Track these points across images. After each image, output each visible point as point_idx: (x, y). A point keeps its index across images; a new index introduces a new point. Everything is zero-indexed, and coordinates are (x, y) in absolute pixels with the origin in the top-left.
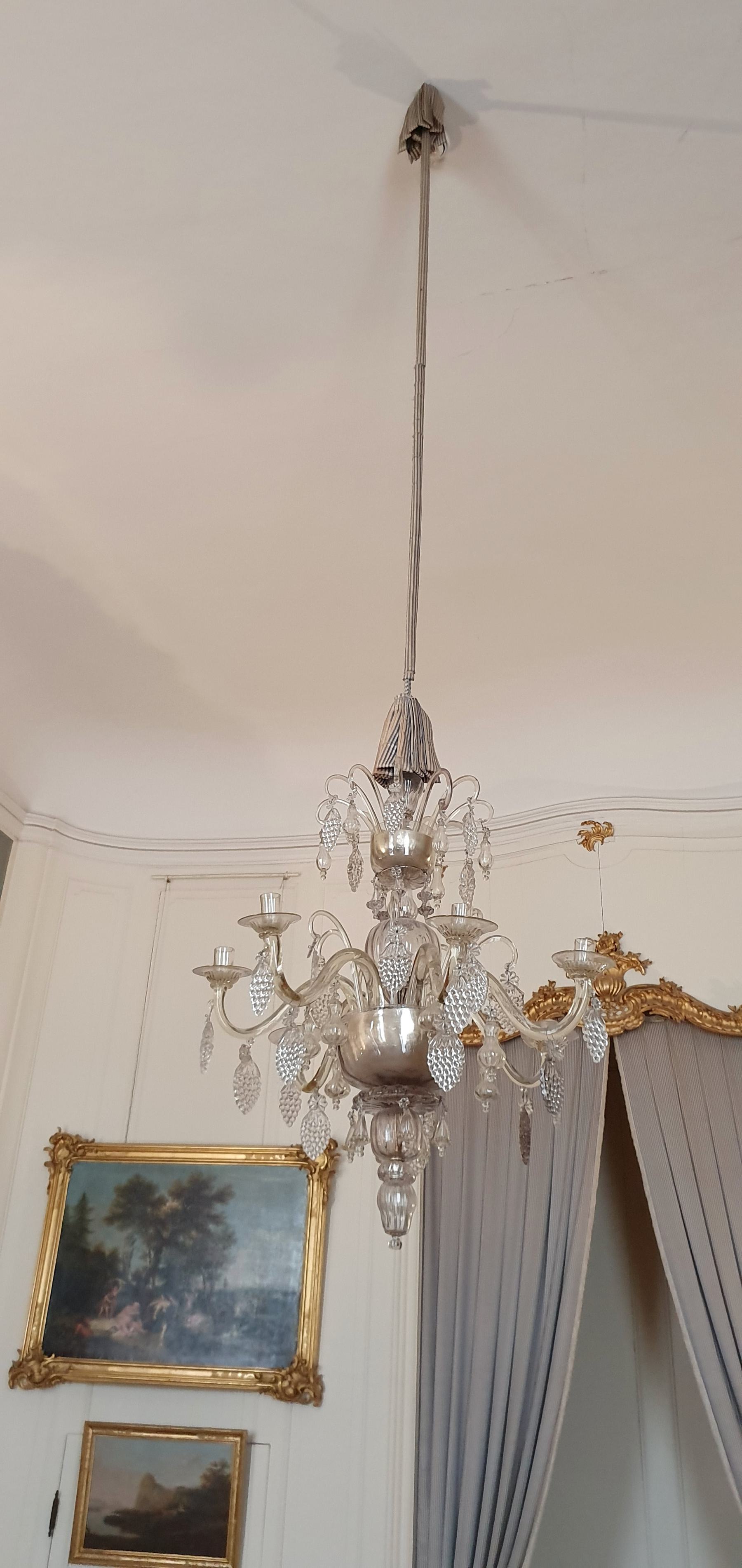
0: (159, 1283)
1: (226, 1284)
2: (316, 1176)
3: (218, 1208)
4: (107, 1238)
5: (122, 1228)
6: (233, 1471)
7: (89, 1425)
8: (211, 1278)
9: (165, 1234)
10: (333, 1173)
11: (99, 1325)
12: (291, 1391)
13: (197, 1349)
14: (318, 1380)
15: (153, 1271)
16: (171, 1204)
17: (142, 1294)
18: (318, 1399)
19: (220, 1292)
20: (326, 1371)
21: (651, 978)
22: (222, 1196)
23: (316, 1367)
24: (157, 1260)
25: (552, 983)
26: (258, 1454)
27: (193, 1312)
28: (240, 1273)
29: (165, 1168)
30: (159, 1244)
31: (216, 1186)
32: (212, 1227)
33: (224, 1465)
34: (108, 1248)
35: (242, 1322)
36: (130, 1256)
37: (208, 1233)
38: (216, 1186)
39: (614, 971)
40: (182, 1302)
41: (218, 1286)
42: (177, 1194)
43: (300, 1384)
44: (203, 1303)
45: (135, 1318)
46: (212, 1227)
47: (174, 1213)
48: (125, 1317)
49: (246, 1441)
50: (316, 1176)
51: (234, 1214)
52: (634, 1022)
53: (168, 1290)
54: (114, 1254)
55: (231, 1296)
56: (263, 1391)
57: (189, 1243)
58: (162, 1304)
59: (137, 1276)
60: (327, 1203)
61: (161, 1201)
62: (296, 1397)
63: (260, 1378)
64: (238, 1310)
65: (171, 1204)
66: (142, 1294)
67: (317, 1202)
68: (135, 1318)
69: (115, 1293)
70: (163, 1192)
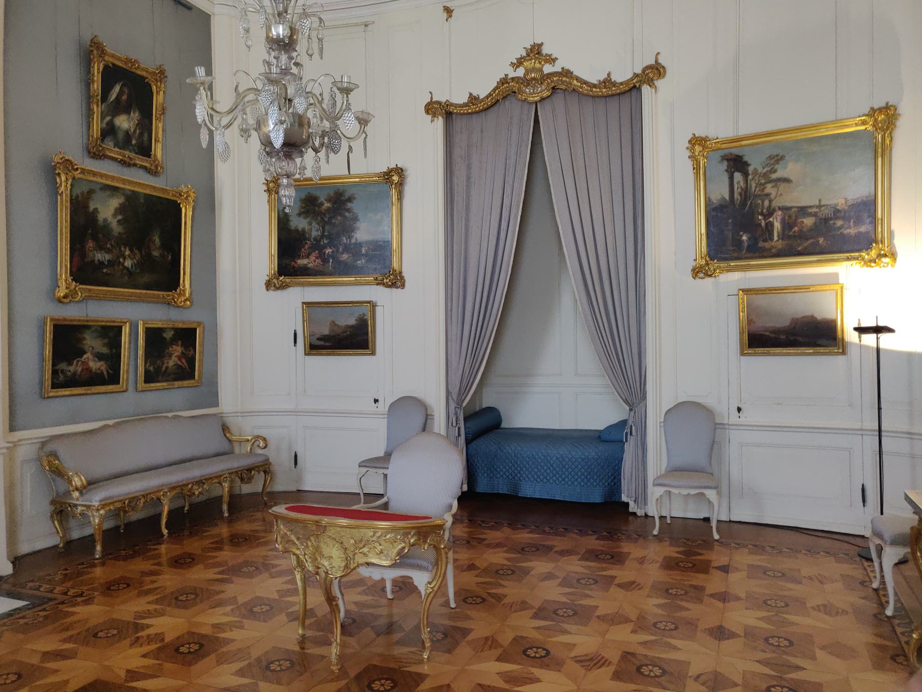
3: (349, 205)
4: (299, 223)
6: (368, 317)
7: (303, 303)
8: (350, 237)
9: (326, 219)
11: (302, 262)
13: (345, 269)
14: (402, 278)
15: (323, 236)
16: (327, 205)
17: (317, 246)
19: (356, 244)
21: (557, 68)
22: (350, 200)
23: (401, 273)
25: (506, 75)
26: (379, 310)
27: (342, 253)
28: (363, 233)
30: (323, 224)
31: (347, 195)
32: (347, 214)
33: (364, 315)
35: (366, 255)
38: (347, 195)
39: (537, 65)
41: (353, 241)
42: (329, 200)
43: (395, 280)
44: (347, 249)
46: (347, 214)
47: (328, 209)
48: (312, 258)
49: (373, 305)
51: (355, 206)
52: (546, 94)
53: (330, 245)
54: (303, 230)
55: (359, 245)
56: (378, 284)
58: (328, 251)
59: (315, 239)
60: (400, 198)
61: (322, 204)
62: (393, 285)
63: (376, 279)
64: (363, 251)
65: (327, 205)
66: (317, 246)
67: (395, 198)
68: (317, 258)
69: (306, 247)
70: (322, 199)
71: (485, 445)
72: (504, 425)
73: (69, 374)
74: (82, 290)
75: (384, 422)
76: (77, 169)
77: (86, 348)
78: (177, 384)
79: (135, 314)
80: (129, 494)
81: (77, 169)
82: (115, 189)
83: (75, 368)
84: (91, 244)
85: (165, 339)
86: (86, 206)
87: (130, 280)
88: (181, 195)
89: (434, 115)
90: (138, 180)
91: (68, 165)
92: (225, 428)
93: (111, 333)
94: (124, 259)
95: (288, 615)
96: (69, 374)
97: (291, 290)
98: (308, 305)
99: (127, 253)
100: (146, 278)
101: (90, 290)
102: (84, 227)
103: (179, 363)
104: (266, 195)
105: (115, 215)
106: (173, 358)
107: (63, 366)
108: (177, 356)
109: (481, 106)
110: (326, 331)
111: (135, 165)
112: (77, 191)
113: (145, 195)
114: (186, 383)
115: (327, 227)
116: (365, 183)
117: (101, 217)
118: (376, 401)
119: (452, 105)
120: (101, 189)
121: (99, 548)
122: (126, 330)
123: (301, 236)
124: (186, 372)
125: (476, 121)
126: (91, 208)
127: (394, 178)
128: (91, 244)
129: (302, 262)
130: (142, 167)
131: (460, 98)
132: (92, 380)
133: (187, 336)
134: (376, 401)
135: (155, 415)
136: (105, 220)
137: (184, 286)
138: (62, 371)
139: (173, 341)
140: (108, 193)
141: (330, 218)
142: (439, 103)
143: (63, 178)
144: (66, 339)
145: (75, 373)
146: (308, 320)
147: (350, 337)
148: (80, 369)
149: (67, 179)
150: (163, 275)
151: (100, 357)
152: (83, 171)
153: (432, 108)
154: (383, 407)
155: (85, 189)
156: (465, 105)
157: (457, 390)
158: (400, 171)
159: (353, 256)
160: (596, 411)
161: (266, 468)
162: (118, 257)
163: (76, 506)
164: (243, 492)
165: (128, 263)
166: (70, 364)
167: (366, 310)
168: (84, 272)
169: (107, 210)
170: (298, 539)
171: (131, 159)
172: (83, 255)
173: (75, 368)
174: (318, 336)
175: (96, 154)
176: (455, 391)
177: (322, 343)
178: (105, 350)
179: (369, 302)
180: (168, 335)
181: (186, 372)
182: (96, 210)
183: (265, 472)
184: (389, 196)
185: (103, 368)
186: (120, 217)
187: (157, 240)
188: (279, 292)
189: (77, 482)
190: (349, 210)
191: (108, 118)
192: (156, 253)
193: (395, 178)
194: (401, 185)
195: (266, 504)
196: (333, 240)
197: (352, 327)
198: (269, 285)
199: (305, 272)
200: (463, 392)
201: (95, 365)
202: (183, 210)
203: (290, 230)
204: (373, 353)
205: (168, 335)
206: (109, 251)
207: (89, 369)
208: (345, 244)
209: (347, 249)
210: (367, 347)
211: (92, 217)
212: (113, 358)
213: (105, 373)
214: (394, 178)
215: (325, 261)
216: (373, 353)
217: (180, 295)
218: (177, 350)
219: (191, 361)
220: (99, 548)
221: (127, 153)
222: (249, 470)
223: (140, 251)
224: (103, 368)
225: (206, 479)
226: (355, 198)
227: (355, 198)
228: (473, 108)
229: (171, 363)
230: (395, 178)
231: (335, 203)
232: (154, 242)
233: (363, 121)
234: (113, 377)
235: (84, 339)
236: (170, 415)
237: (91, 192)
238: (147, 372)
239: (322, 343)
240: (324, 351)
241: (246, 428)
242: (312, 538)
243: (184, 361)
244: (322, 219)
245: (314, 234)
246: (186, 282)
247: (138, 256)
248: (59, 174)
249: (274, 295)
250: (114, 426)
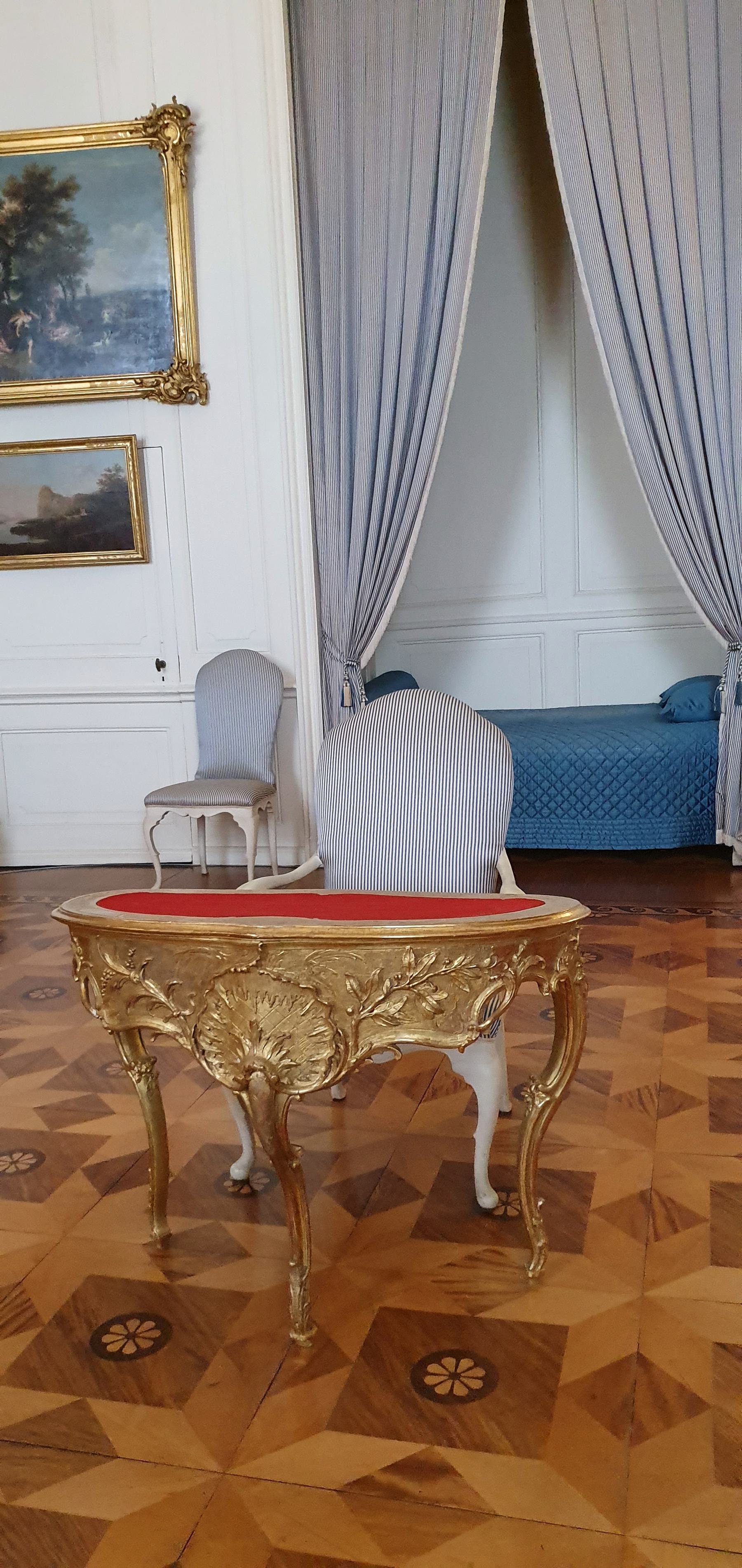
1: (88, 290)
2: (169, 153)
6: (127, 473)
10: (187, 147)
12: (174, 392)
14: (202, 378)
18: (204, 397)
23: (197, 366)
26: (151, 457)
28: (102, 275)
33: (118, 469)
35: (113, 327)
43: (185, 385)
49: (136, 447)
50: (169, 153)
55: (95, 303)
56: (146, 395)
62: (182, 397)
64: (106, 316)
75: (190, 708)
95: (93, 1173)
118: (160, 665)
127: (170, 130)
134: (160, 665)
154: (184, 676)
157: (346, 633)
158: (180, 114)
167: (118, 459)
170: (169, 990)
176: (342, 635)
179: (128, 439)
184: (158, 181)
193: (173, 133)
194: (187, 148)
197: (92, 498)
200: (360, 633)
204: (145, 559)
210: (129, 545)
214: (170, 130)
216: (145, 559)
230: (173, 133)
242: (220, 987)
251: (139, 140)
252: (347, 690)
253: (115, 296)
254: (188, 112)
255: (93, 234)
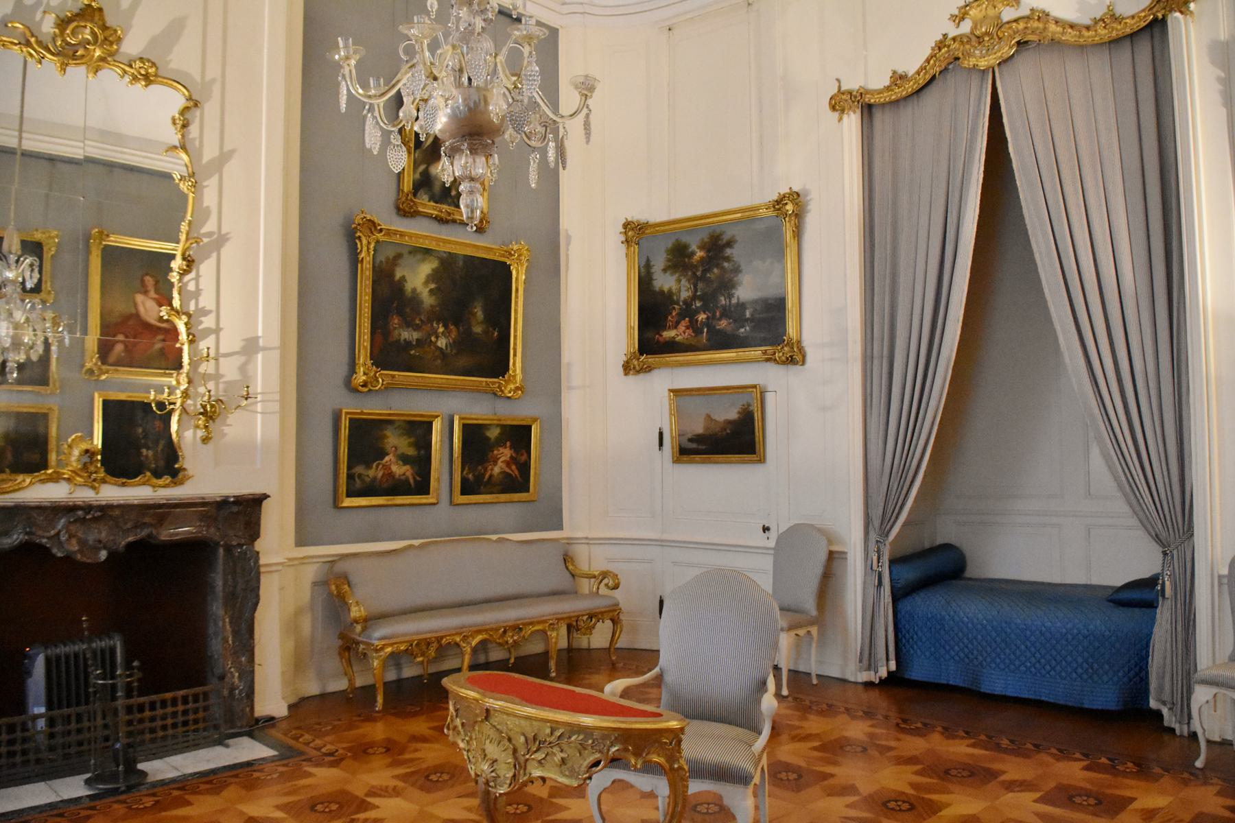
0: (698, 304)
3: (728, 251)
4: (665, 282)
5: (672, 274)
6: (755, 408)
7: (671, 391)
8: (730, 296)
9: (699, 273)
11: (669, 334)
13: (723, 342)
15: (694, 298)
16: (700, 254)
20: (806, 343)
22: (729, 244)
23: (799, 342)
24: (696, 291)
26: (770, 398)
27: (720, 319)
28: (747, 290)
29: (692, 231)
30: (695, 280)
34: (666, 289)
35: (752, 320)
36: (680, 291)
37: (723, 268)
38: (726, 238)
40: (714, 315)
41: (734, 301)
42: (701, 248)
44: (726, 313)
45: (688, 328)
46: (726, 264)
47: (702, 258)
48: (682, 327)
49: (761, 393)
51: (734, 252)
53: (705, 309)
54: (670, 291)
55: (742, 306)
56: (768, 360)
57: (713, 276)
58: (702, 317)
59: (685, 302)
60: (798, 233)
61: (693, 253)
62: (791, 361)
63: (765, 353)
64: (748, 314)
65: (700, 254)
66: (688, 312)
68: (688, 328)
70: (694, 247)
71: (928, 604)
72: (971, 572)
73: (367, 479)
74: (385, 376)
76: (381, 230)
77: (388, 447)
78: (504, 497)
79: (449, 406)
80: (417, 634)
81: (381, 230)
82: (427, 252)
83: (374, 473)
84: (396, 321)
85: (488, 439)
86: (391, 275)
87: (445, 363)
88: (511, 255)
89: (843, 111)
90: (463, 242)
91: (372, 226)
92: (567, 559)
93: (419, 430)
94: (437, 337)
96: (367, 479)
97: (656, 373)
98: (677, 393)
99: (441, 330)
100: (463, 361)
101: (393, 376)
102: (390, 300)
103: (507, 470)
104: (624, 247)
105: (426, 283)
106: (500, 463)
107: (359, 469)
108: (503, 462)
109: (910, 87)
110: (699, 429)
111: (454, 221)
112: (381, 258)
113: (466, 256)
114: (516, 496)
115: (700, 285)
116: (748, 217)
117: (409, 287)
118: (766, 529)
119: (868, 92)
120: (410, 253)
121: (380, 699)
122: (437, 426)
123: (667, 298)
124: (517, 482)
125: (907, 112)
126: (398, 275)
127: (790, 208)
128: (396, 321)
129: (669, 334)
130: (429, 216)
131: (877, 80)
132: (396, 488)
133: (519, 435)
134: (766, 529)
135: (476, 534)
136: (414, 290)
137: (515, 371)
138: (360, 476)
139: (500, 442)
140: (419, 256)
141: (705, 271)
142: (850, 93)
143: (365, 242)
144: (364, 439)
145: (375, 478)
146: (678, 413)
147: (732, 438)
148: (380, 474)
149: (369, 243)
150: (488, 357)
151: (405, 459)
152: (389, 233)
153: (838, 104)
155: (390, 253)
156: (888, 88)
158: (795, 197)
159: (735, 321)
160: (1125, 558)
161: (614, 615)
162: (429, 335)
163: (358, 643)
164: (593, 646)
165: (442, 343)
166: (369, 467)
168: (389, 355)
169: (417, 278)
171: (449, 214)
172: (387, 333)
173: (374, 473)
174: (689, 436)
175: (405, 210)
177: (694, 446)
178: (411, 452)
179: (755, 387)
180: (493, 434)
181: (517, 482)
182: (403, 279)
183: (612, 620)
185: (409, 474)
186: (433, 286)
187: (479, 314)
188: (641, 376)
189: (355, 612)
190: (728, 259)
191: (422, 168)
192: (478, 329)
194: (799, 216)
195: (613, 664)
196: (708, 300)
198: (627, 368)
199: (673, 347)
201: (399, 470)
202: (514, 273)
203: (654, 292)
204: (762, 460)
205: (493, 434)
206: (417, 328)
207: (391, 475)
208: (724, 308)
209: (726, 313)
211: (398, 288)
212: (422, 462)
213: (412, 481)
215: (698, 332)
217: (507, 382)
218: (505, 453)
219: (525, 468)
220: (380, 699)
221: (445, 207)
222: (591, 617)
223: (456, 325)
224: (409, 474)
225: (524, 624)
226: (735, 241)
227: (735, 241)
228: (898, 93)
229: (497, 470)
230: (790, 207)
231: (709, 251)
232: (474, 314)
233: (587, 88)
234: (422, 487)
235: (385, 437)
236: (494, 537)
237: (399, 256)
238: (464, 481)
239: (694, 446)
240: (697, 457)
241: (592, 560)
243: (514, 467)
244: (694, 274)
245: (685, 295)
246: (516, 363)
247: (454, 334)
248: (359, 238)
249: (632, 379)
250: (422, 546)
251: (771, 213)
252: (875, 558)
253: (755, 302)
254: (798, 195)
255: (743, 267)
